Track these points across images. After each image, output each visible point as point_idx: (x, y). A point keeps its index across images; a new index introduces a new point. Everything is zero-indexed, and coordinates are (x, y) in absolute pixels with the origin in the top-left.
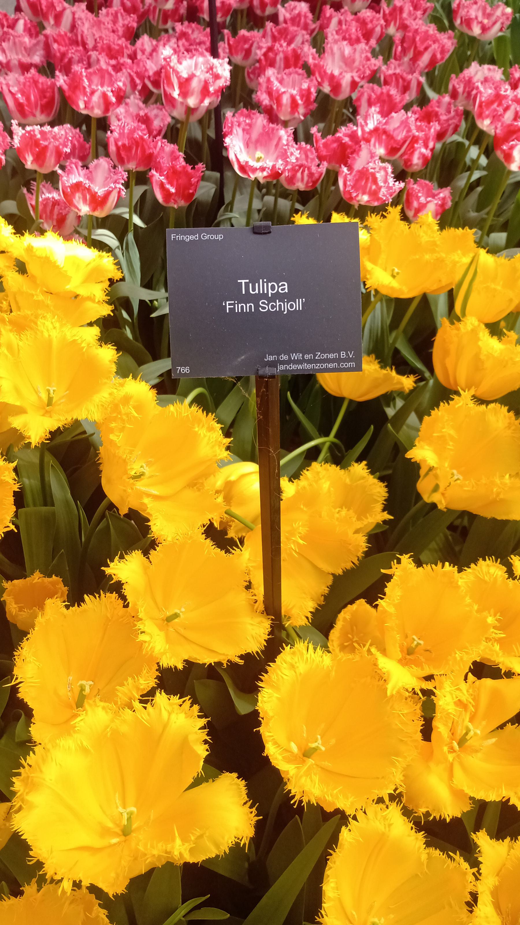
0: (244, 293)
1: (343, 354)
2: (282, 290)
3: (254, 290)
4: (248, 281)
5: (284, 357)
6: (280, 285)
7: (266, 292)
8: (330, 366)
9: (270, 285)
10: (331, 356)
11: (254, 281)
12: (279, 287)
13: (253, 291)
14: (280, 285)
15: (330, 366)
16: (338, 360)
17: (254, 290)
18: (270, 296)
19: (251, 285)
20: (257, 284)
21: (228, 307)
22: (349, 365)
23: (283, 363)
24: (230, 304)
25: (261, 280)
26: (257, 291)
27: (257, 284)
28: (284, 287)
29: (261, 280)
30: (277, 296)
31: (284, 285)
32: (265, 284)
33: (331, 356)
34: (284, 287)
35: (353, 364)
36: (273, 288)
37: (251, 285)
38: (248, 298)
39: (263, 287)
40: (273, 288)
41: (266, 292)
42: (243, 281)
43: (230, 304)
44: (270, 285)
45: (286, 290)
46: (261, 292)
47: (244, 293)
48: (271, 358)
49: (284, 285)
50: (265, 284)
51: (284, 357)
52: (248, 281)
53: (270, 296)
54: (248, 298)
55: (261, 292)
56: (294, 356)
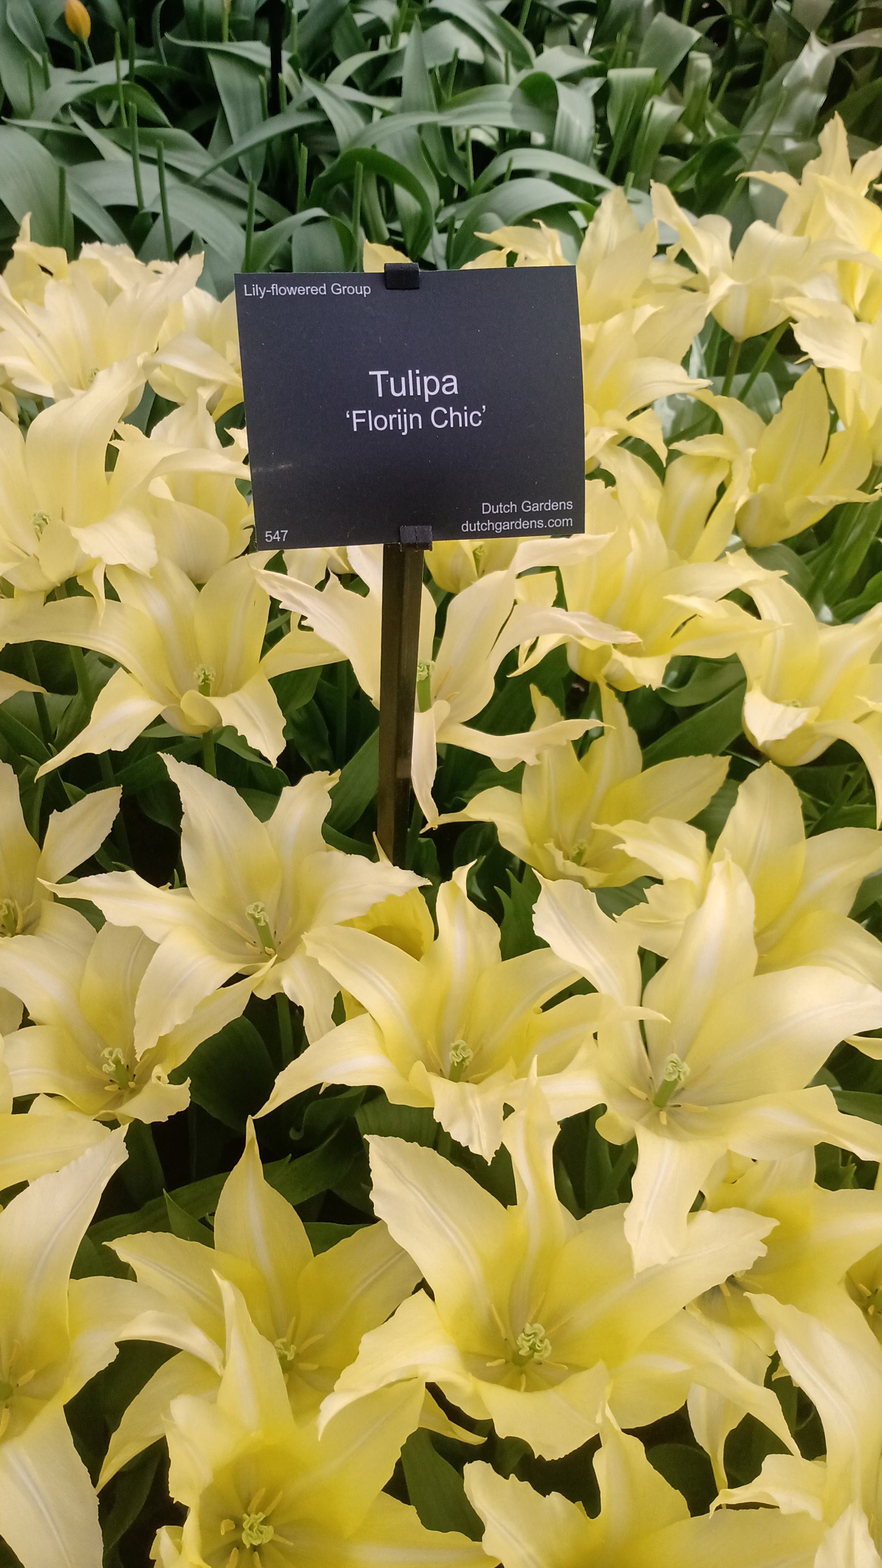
0: (380, 395)
1: (553, 506)
2: (448, 389)
3: (398, 390)
4: (387, 372)
6: (444, 380)
7: (419, 394)
9: (426, 379)
11: (398, 373)
12: (442, 384)
13: (396, 392)
14: (444, 380)
16: (544, 515)
17: (398, 390)
18: (427, 400)
19: (392, 379)
20: (403, 379)
21: (355, 421)
22: (562, 522)
24: (358, 416)
25: (410, 372)
26: (404, 392)
27: (403, 379)
29: (410, 372)
31: (450, 380)
32: (418, 378)
34: (451, 385)
37: (392, 379)
39: (416, 384)
41: (419, 394)
42: (379, 374)
43: (358, 416)
44: (426, 379)
45: (455, 390)
46: (412, 394)
47: (380, 395)
49: (450, 380)
50: (418, 378)
52: (387, 372)
53: (427, 400)
54: (388, 405)
55: (412, 394)
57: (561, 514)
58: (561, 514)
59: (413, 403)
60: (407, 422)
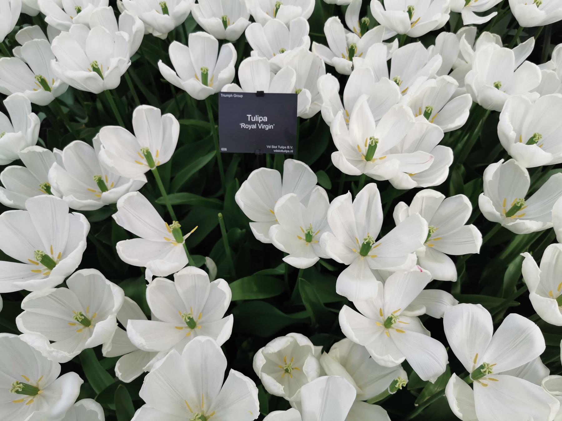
11: (254, 116)
28: (265, 119)
30: (263, 123)
34: (265, 119)
36: (261, 119)
39: (257, 118)
40: (261, 119)
42: (249, 116)
54: (251, 123)
57: (290, 150)
58: (290, 150)
59: (257, 122)
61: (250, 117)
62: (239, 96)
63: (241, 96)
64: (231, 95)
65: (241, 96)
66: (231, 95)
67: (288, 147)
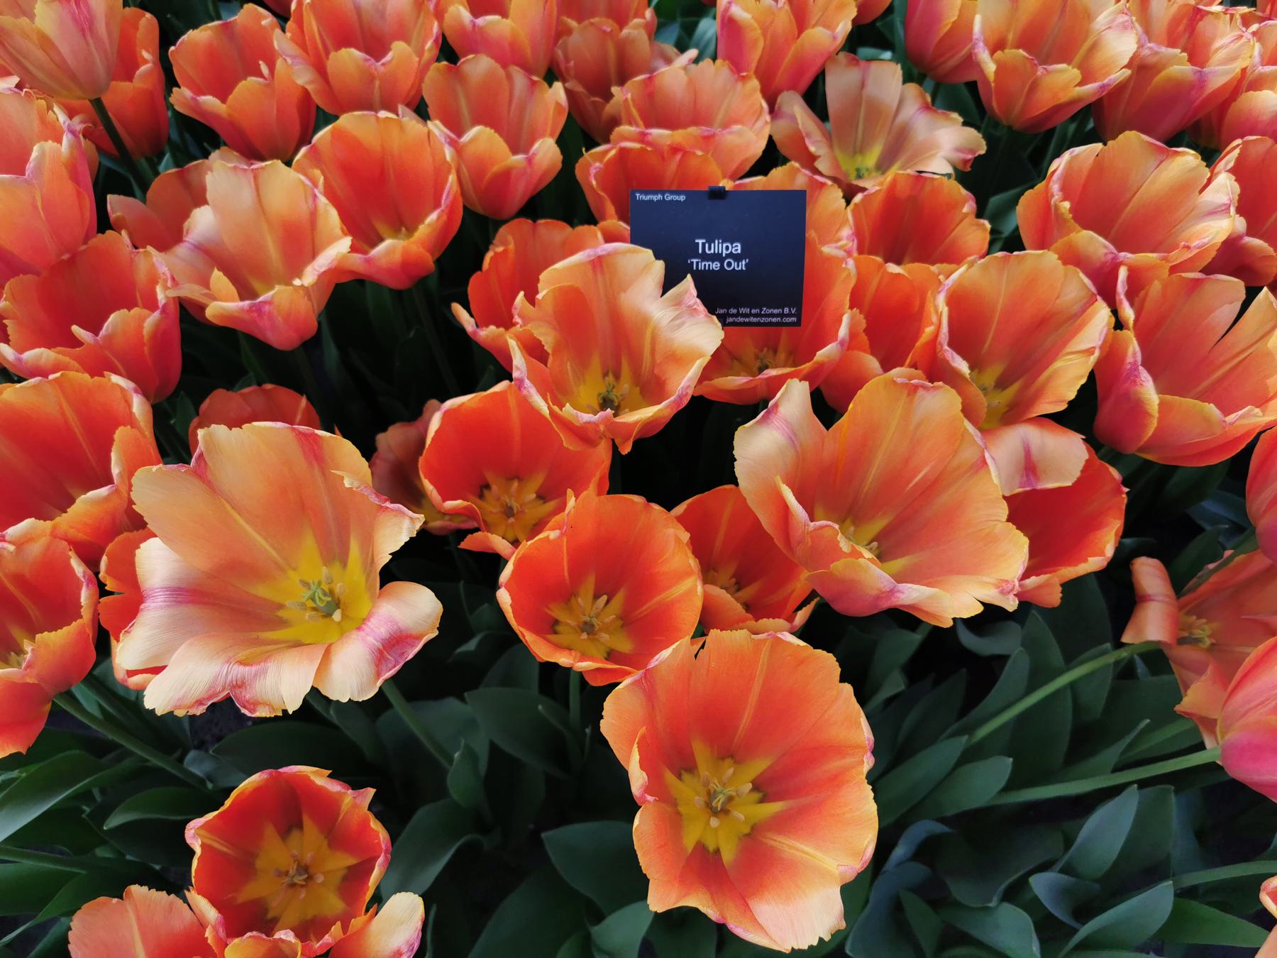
5: (733, 311)
8: (774, 320)
10: (776, 311)
11: (710, 241)
15: (774, 320)
16: (782, 315)
23: (733, 315)
28: (737, 248)
33: (776, 311)
34: (737, 248)
35: (794, 319)
36: (727, 248)
38: (705, 257)
39: (719, 247)
40: (727, 248)
42: (700, 242)
48: (722, 311)
51: (733, 311)
54: (705, 257)
56: (743, 310)
59: (717, 257)
60: (715, 266)
61: (704, 244)
62: (676, 198)
63: (682, 198)
64: (660, 197)
65: (682, 198)
66: (660, 197)
67: (786, 310)
